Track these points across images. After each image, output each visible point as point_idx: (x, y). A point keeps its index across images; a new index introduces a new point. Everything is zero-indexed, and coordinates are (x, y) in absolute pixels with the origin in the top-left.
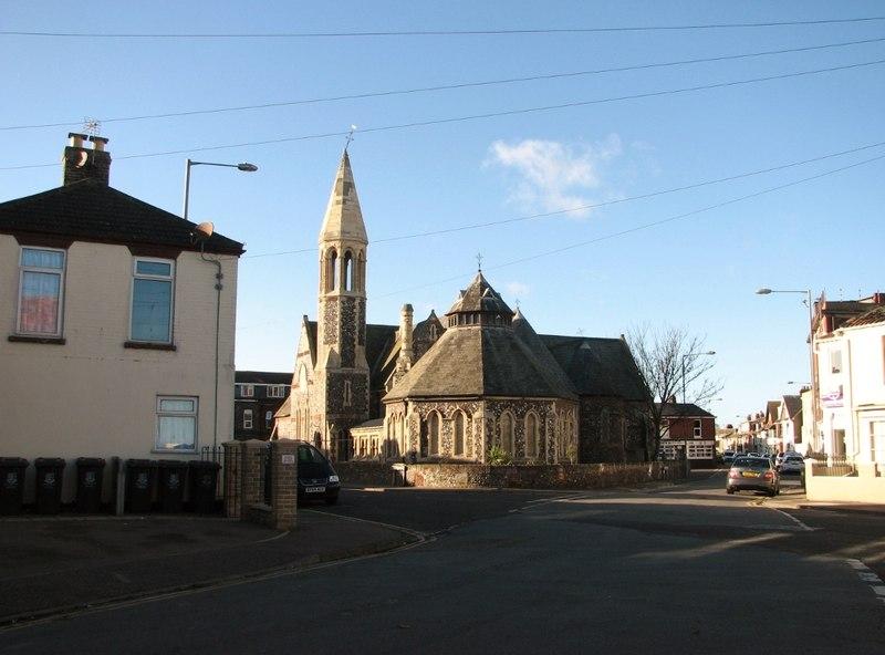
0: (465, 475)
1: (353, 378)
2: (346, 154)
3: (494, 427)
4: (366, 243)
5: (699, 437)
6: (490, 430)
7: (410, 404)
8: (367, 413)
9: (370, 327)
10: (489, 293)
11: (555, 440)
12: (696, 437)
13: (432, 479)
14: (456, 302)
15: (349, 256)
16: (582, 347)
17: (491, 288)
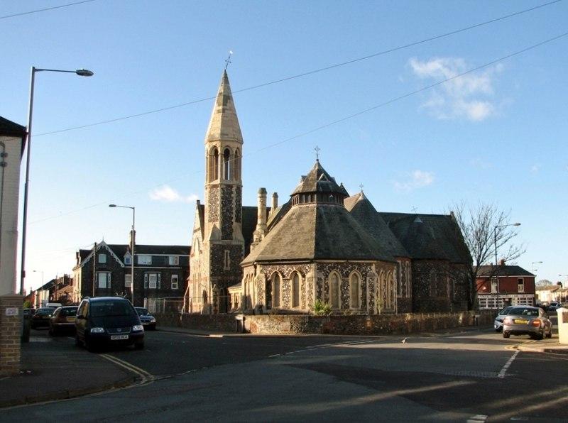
0: (288, 324)
2: (226, 74)
3: (323, 284)
4: (241, 142)
6: (320, 287)
7: (258, 266)
9: (245, 208)
10: (323, 177)
11: (375, 295)
13: (263, 327)
14: (298, 185)
15: (227, 155)
16: (416, 221)
17: (326, 174)
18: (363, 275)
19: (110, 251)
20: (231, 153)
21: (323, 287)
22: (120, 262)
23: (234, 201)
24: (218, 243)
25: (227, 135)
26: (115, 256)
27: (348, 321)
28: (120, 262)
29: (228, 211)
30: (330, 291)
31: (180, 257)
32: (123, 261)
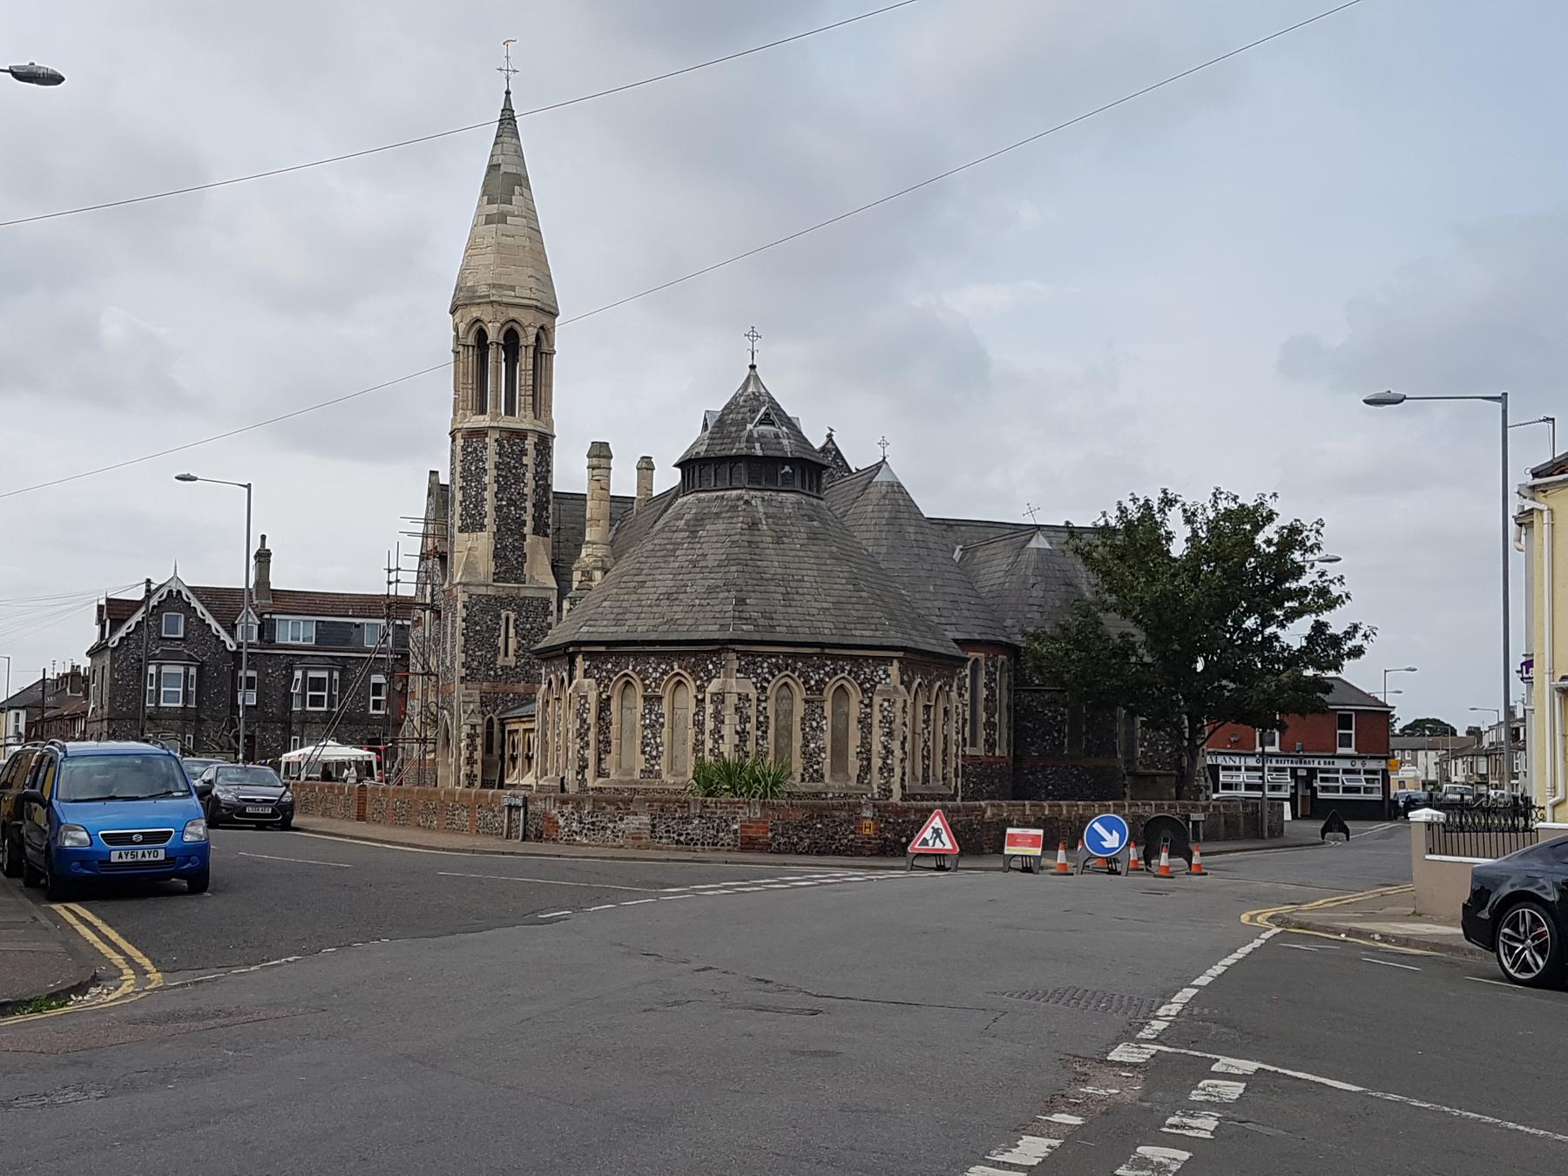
0: (646, 819)
2: (508, 119)
5: (1351, 751)
6: (745, 720)
7: (579, 659)
10: (766, 414)
11: (896, 746)
12: (1340, 751)
14: (686, 436)
15: (505, 347)
16: (1033, 544)
18: (864, 691)
19: (195, 603)
20: (522, 342)
21: (754, 720)
22: (224, 636)
23: (529, 475)
24: (482, 591)
25: (513, 288)
26: (210, 620)
27: (811, 817)
28: (224, 636)
29: (511, 502)
30: (771, 732)
32: (231, 631)
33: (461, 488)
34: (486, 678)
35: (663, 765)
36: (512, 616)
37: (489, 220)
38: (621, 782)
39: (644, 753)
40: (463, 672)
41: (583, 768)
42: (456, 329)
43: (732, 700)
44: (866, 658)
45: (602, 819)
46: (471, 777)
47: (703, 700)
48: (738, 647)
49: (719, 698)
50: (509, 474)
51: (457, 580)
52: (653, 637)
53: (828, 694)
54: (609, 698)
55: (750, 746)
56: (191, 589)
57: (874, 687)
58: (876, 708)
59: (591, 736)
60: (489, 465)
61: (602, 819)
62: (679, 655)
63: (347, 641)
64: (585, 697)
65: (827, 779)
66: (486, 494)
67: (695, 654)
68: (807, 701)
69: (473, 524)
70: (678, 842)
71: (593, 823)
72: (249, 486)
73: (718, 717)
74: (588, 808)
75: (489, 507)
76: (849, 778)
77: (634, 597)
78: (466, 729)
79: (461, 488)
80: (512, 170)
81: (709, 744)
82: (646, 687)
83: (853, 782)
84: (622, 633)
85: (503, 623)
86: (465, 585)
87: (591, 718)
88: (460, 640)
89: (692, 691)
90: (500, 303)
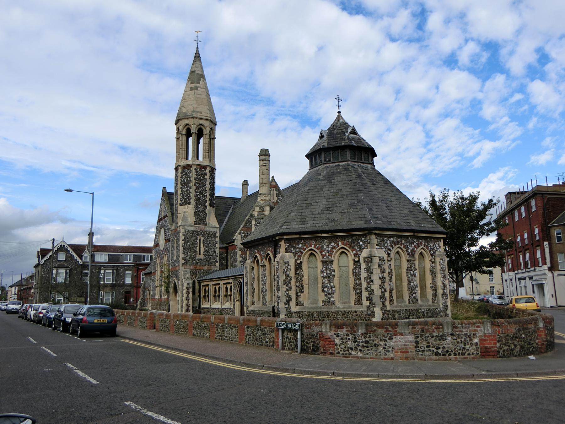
0: (411, 338)
1: (205, 234)
2: (197, 56)
3: (386, 267)
4: (215, 124)
6: (383, 271)
7: (282, 243)
8: (217, 264)
13: (350, 344)
18: (432, 255)
19: (69, 249)
20: (205, 132)
22: (78, 259)
24: (190, 228)
25: (201, 113)
26: (74, 254)
27: (519, 330)
28: (78, 259)
29: (201, 193)
30: (394, 277)
31: (134, 255)
32: (81, 257)
33: (181, 188)
34: (192, 264)
35: (336, 298)
36: (202, 238)
37: (191, 89)
38: (311, 308)
39: (323, 291)
40: (183, 262)
41: (288, 301)
42: (178, 129)
43: (376, 260)
44: (431, 238)
45: (374, 340)
46: (188, 305)
47: (359, 261)
48: (378, 232)
49: (369, 259)
50: (200, 183)
51: (179, 224)
52: (327, 228)
53: (417, 256)
54: (301, 262)
55: (387, 286)
56: (69, 245)
57: (435, 253)
58: (438, 263)
59: (293, 283)
60: (192, 179)
61: (374, 340)
62: (342, 237)
63: (118, 261)
64: (288, 263)
65: (419, 302)
66: (191, 190)
67: (351, 236)
68: (408, 261)
69: (186, 202)
70: (437, 354)
71: (366, 342)
72: (93, 194)
73: (369, 270)
74: (361, 331)
75: (192, 195)
76: (428, 300)
77: (307, 210)
78: (185, 285)
79: (181, 188)
80: (199, 72)
81: (364, 285)
82: (323, 256)
83: (430, 303)
84: (307, 227)
85: (198, 241)
86: (184, 226)
87: (292, 274)
88: (181, 249)
89: (351, 256)
90: (196, 118)
